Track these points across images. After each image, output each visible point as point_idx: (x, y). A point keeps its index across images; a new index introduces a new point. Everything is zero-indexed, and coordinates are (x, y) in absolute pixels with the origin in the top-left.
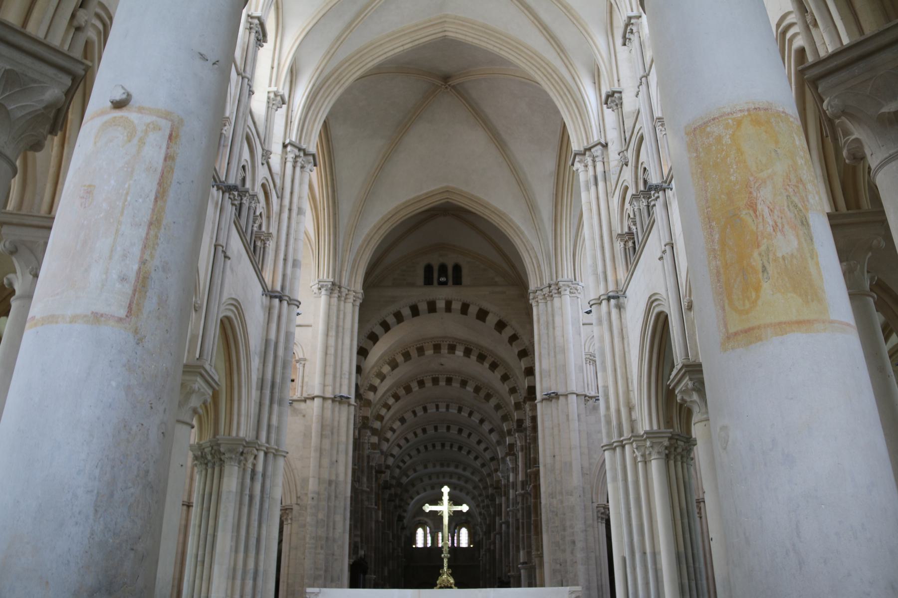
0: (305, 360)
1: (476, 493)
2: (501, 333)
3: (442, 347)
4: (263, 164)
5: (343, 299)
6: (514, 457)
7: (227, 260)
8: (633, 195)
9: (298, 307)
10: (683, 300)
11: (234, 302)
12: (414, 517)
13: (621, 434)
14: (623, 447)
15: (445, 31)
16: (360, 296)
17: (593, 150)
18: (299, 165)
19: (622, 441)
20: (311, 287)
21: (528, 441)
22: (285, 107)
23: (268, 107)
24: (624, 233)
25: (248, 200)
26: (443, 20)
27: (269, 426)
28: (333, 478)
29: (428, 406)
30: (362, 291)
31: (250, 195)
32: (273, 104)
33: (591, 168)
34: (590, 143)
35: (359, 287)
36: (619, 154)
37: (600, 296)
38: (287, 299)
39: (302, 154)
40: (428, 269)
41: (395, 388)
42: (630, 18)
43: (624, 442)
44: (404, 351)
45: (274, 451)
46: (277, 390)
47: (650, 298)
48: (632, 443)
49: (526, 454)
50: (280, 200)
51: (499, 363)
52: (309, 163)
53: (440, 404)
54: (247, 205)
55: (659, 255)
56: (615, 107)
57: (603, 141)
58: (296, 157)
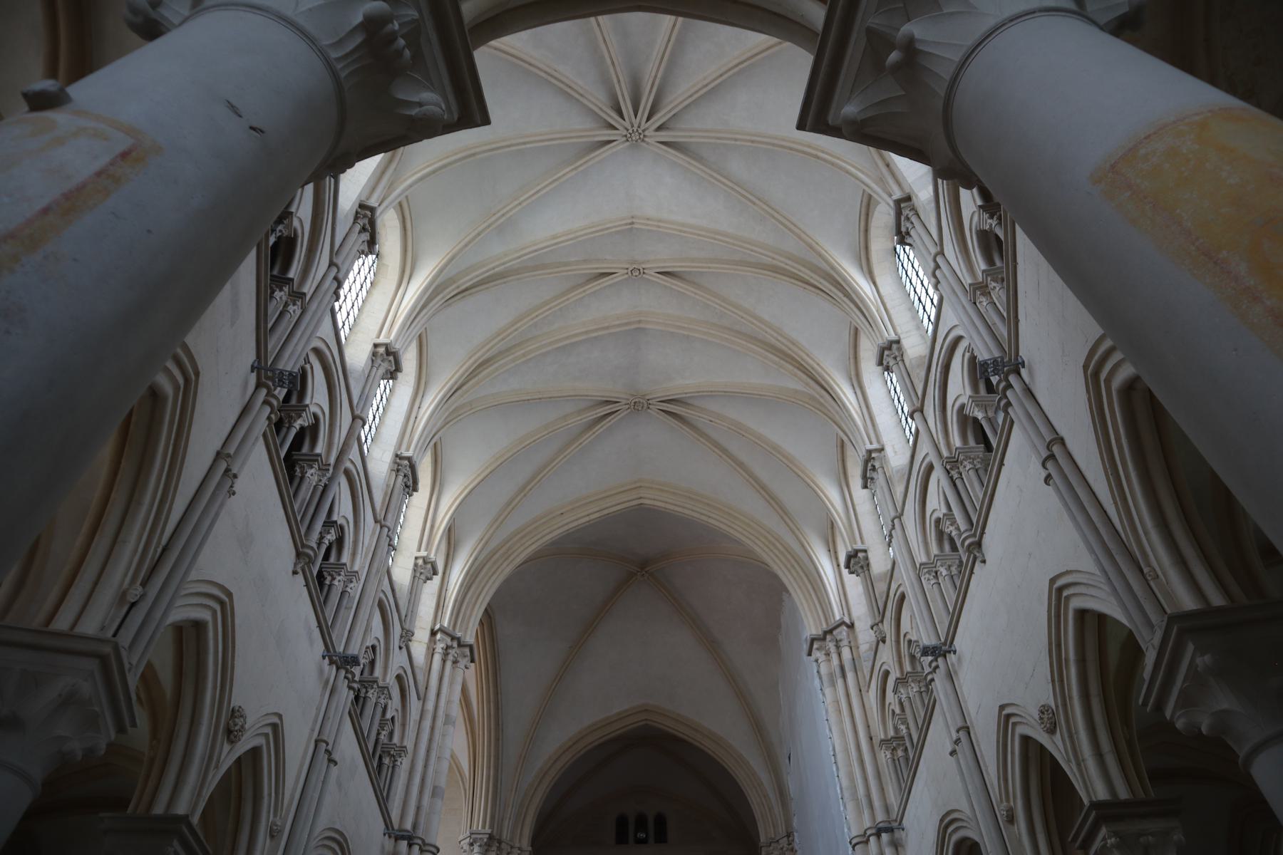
4: (400, 648)
7: (332, 765)
8: (897, 679)
10: (998, 808)
11: (337, 836)
15: (641, 498)
17: (835, 633)
18: (450, 658)
20: (460, 842)
22: (437, 579)
23: (414, 577)
24: (889, 737)
25: (376, 694)
26: (638, 485)
30: (530, 849)
31: (378, 687)
32: (421, 573)
33: (834, 657)
34: (830, 624)
36: (872, 629)
37: (866, 830)
38: (420, 842)
39: (455, 644)
40: (622, 822)
42: (870, 452)
47: (942, 821)
50: (421, 702)
52: (465, 656)
54: (374, 700)
55: (949, 747)
56: (860, 571)
57: (847, 620)
58: (448, 647)
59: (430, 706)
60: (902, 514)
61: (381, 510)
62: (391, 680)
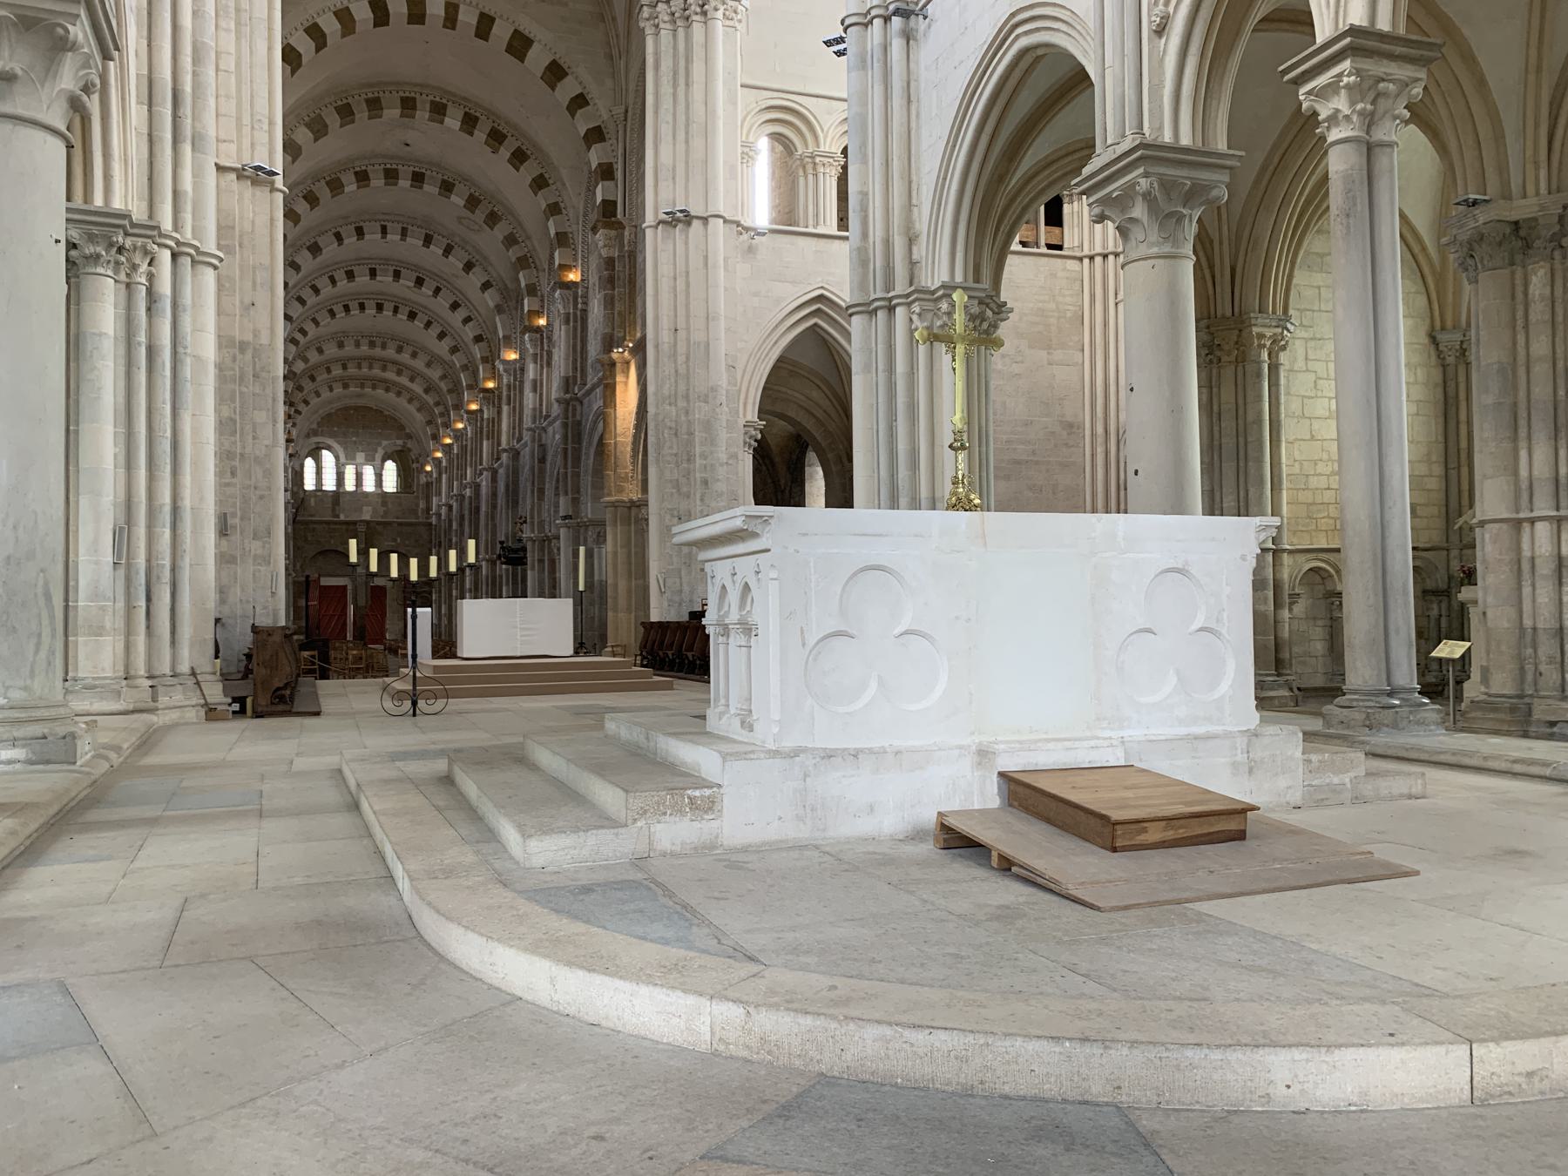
1: (430, 400)
2: (553, 88)
3: (418, 105)
6: (538, 336)
10: (1149, 10)
12: (308, 436)
13: (889, 286)
14: (891, 309)
19: (890, 299)
21: (580, 306)
29: (366, 227)
37: (871, 8)
41: (309, 181)
43: (894, 302)
44: (339, 103)
45: (192, 251)
46: (187, 109)
48: (909, 304)
49: (575, 329)
51: (529, 152)
53: (389, 225)
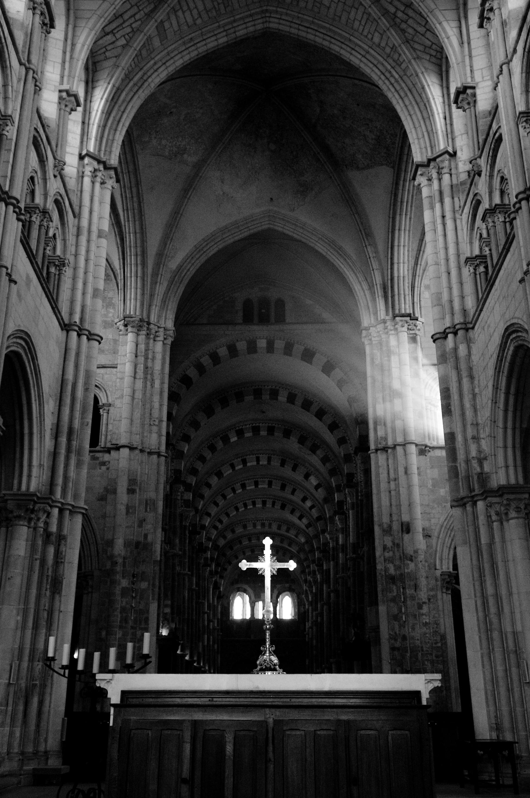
0: (110, 405)
4: (55, 176)
5: (152, 336)
7: (13, 285)
9: (100, 343)
16: (171, 333)
17: (438, 160)
18: (98, 179)
20: (116, 324)
22: (80, 109)
23: (60, 110)
24: (474, 255)
25: (38, 217)
27: (66, 478)
28: (142, 539)
30: (174, 329)
31: (40, 212)
32: (66, 106)
33: (436, 183)
34: (434, 152)
35: (170, 324)
36: (471, 162)
38: (87, 333)
39: (101, 167)
45: (70, 508)
47: (507, 329)
50: (77, 220)
52: (111, 178)
54: (38, 223)
55: (519, 276)
56: (466, 107)
57: (450, 150)
58: (95, 170)
59: (85, 223)
60: (511, 60)
61: (24, 46)
62: (51, 206)
